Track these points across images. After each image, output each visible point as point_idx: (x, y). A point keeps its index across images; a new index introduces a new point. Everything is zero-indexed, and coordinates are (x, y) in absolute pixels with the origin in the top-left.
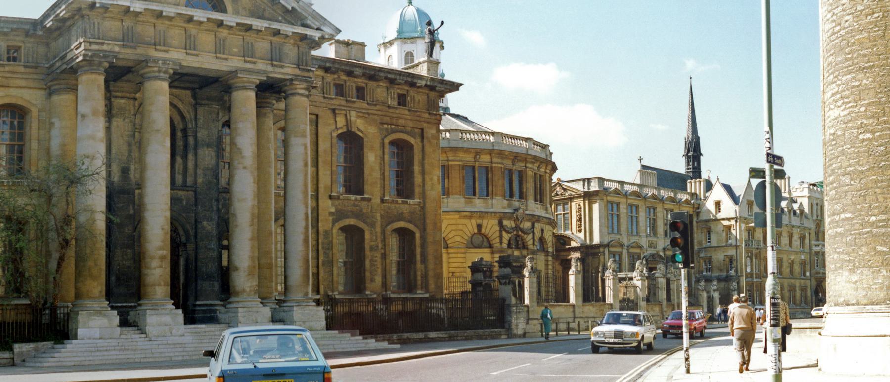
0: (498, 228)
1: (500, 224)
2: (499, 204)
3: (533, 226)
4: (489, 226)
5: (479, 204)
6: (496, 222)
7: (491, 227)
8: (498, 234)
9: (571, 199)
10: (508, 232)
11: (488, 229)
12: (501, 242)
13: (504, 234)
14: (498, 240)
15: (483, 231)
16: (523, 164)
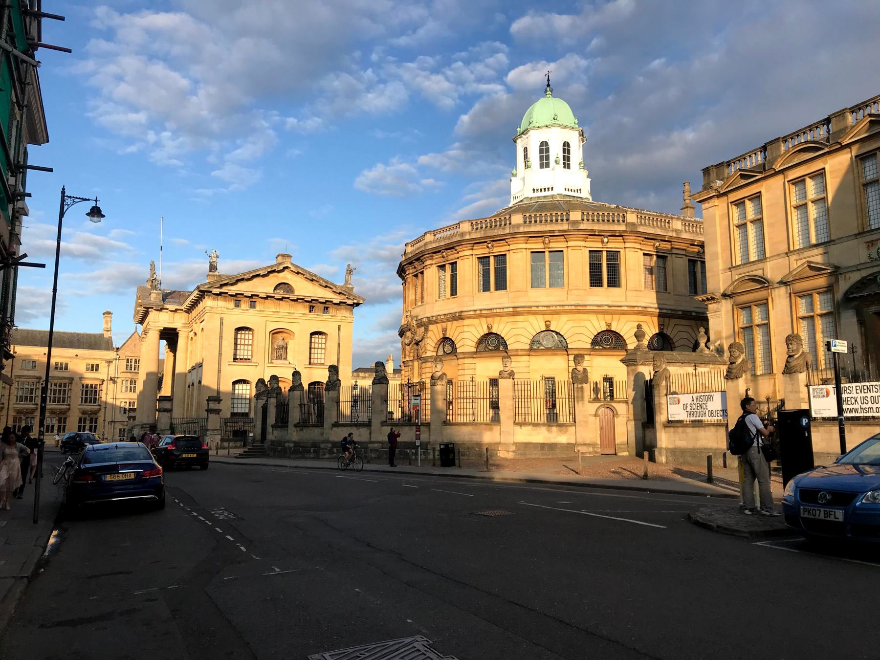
3: (427, 330)
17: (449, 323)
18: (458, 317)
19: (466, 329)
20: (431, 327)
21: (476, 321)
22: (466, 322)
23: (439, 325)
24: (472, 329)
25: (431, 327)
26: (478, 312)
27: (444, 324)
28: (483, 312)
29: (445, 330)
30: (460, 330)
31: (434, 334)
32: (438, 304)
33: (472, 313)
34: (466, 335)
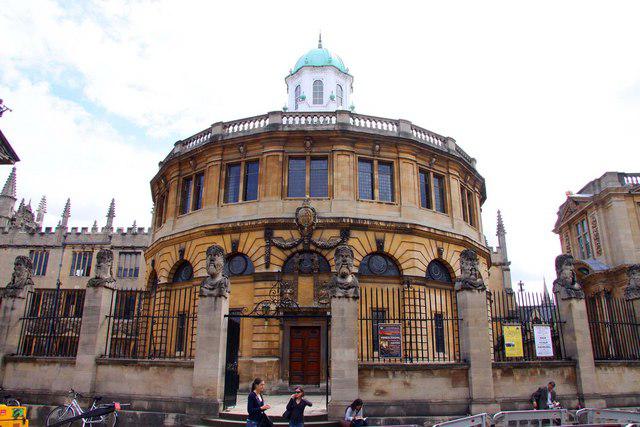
0: (263, 243)
1: (268, 236)
2: (272, 206)
3: (345, 234)
4: (250, 241)
5: (240, 212)
6: (261, 234)
7: (253, 245)
8: (263, 251)
9: (584, 213)
10: (280, 247)
11: (248, 246)
12: (267, 265)
13: (274, 250)
14: (262, 261)
15: (240, 249)
16: (329, 148)
17: (388, 237)
18: (408, 230)
19: (416, 247)
20: (354, 233)
21: (425, 241)
22: (416, 239)
23: (371, 235)
24: (423, 249)
25: (354, 233)
26: (432, 231)
27: (380, 235)
28: (438, 232)
29: (380, 243)
30: (407, 246)
31: (361, 244)
32: (361, 205)
33: (426, 229)
34: (416, 255)
